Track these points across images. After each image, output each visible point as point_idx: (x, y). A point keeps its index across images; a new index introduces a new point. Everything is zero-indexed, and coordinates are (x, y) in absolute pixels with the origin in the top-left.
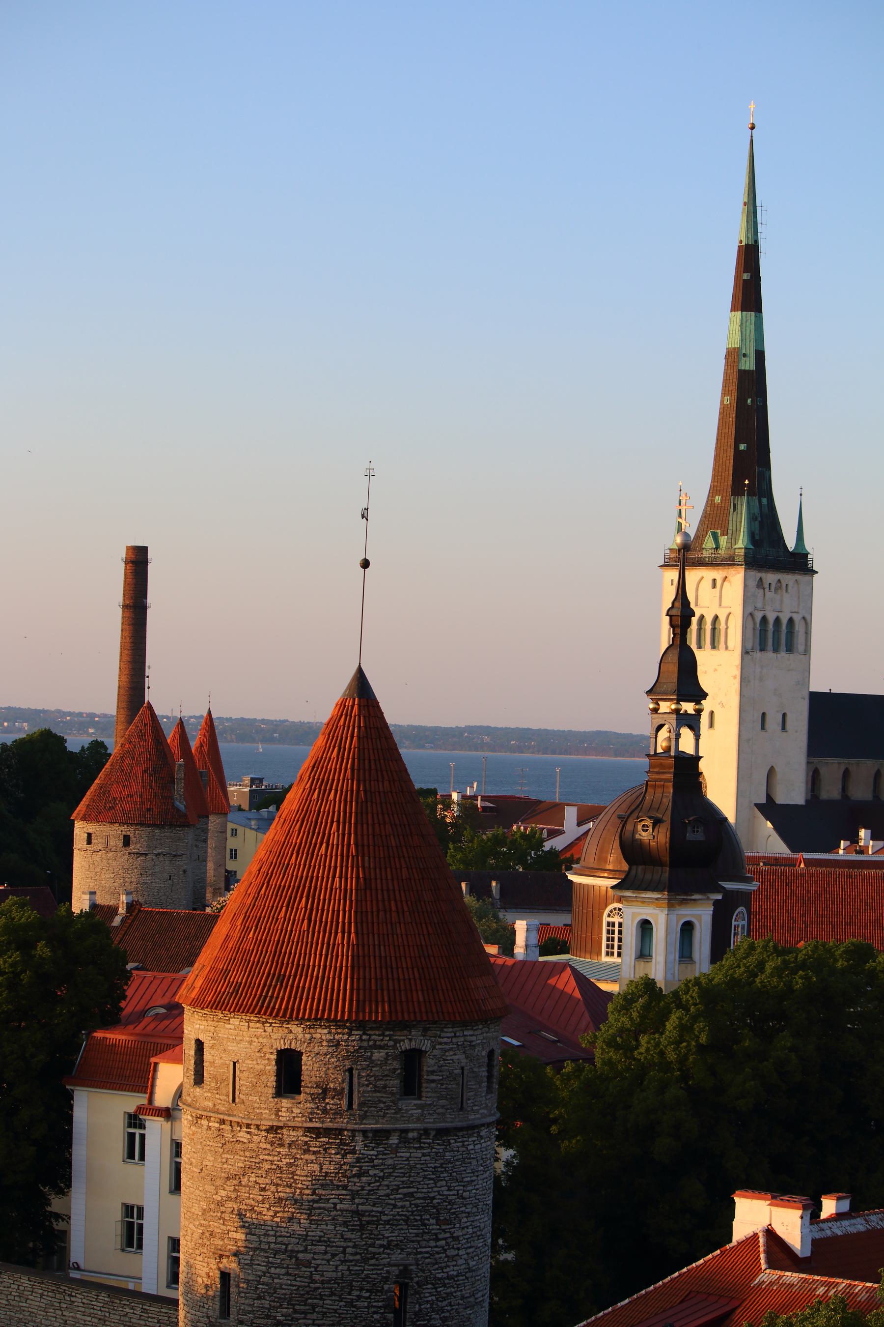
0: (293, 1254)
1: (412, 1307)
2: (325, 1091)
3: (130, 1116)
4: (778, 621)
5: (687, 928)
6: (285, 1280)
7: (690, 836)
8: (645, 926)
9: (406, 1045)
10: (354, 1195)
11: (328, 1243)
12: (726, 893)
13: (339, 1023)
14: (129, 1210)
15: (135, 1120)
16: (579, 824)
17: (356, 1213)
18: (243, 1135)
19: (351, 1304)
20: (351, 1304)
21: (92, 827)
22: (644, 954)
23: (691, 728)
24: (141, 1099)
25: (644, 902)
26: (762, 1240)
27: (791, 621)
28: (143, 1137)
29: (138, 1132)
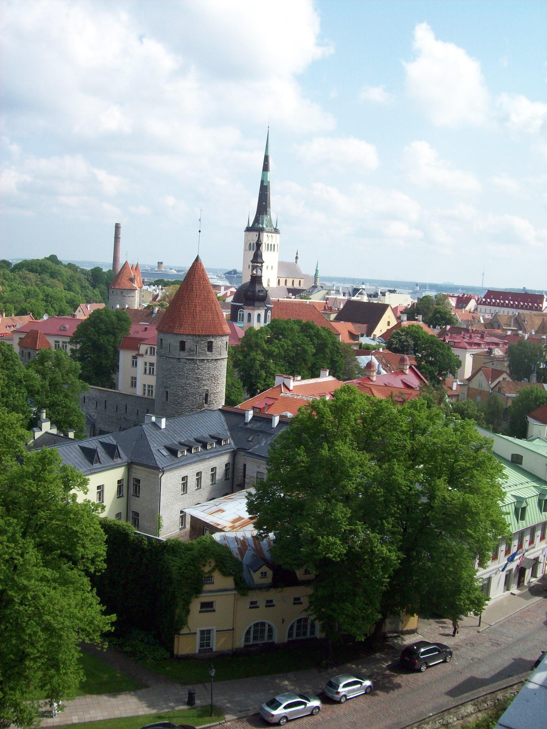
0: (182, 387)
1: (209, 399)
2: (191, 350)
3: (133, 356)
4: (271, 245)
5: (259, 315)
6: (181, 393)
7: (260, 294)
8: (249, 315)
9: (209, 340)
10: (197, 373)
11: (190, 384)
12: (268, 308)
13: (194, 335)
14: (132, 378)
15: (135, 357)
16: (225, 289)
17: (197, 378)
18: (171, 360)
19: (195, 398)
20: (195, 398)
21: (113, 290)
22: (249, 320)
23: (261, 270)
24: (137, 353)
25: (249, 309)
26: (282, 386)
27: (274, 245)
28: (136, 361)
29: (135, 360)
